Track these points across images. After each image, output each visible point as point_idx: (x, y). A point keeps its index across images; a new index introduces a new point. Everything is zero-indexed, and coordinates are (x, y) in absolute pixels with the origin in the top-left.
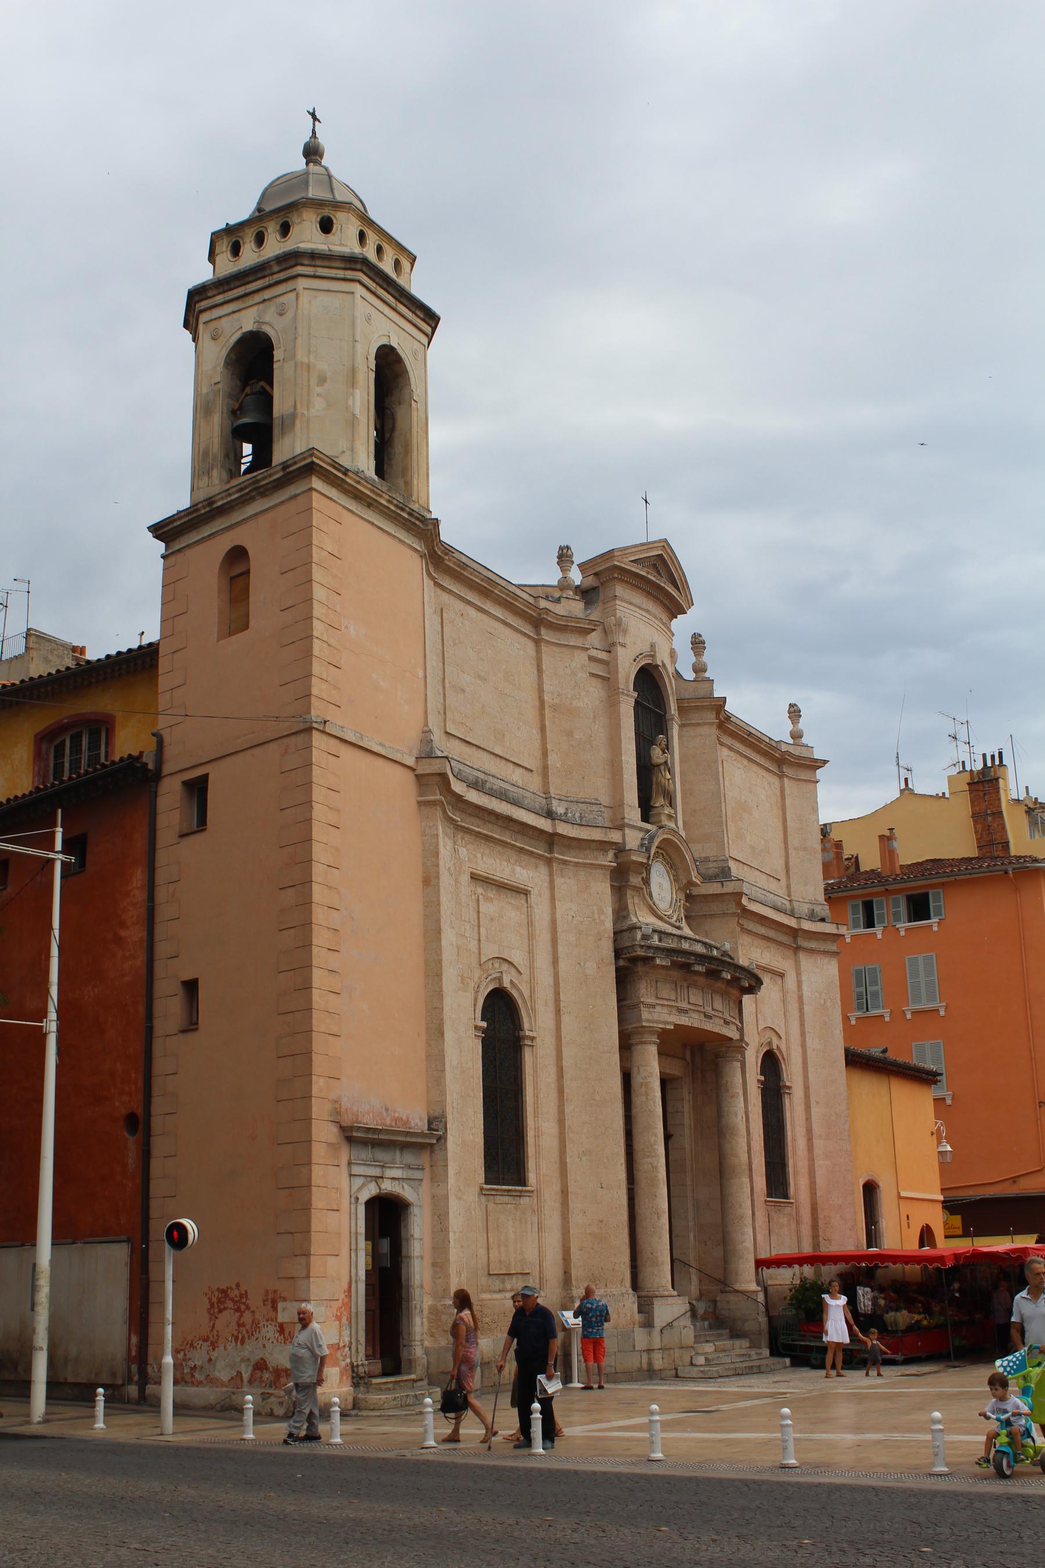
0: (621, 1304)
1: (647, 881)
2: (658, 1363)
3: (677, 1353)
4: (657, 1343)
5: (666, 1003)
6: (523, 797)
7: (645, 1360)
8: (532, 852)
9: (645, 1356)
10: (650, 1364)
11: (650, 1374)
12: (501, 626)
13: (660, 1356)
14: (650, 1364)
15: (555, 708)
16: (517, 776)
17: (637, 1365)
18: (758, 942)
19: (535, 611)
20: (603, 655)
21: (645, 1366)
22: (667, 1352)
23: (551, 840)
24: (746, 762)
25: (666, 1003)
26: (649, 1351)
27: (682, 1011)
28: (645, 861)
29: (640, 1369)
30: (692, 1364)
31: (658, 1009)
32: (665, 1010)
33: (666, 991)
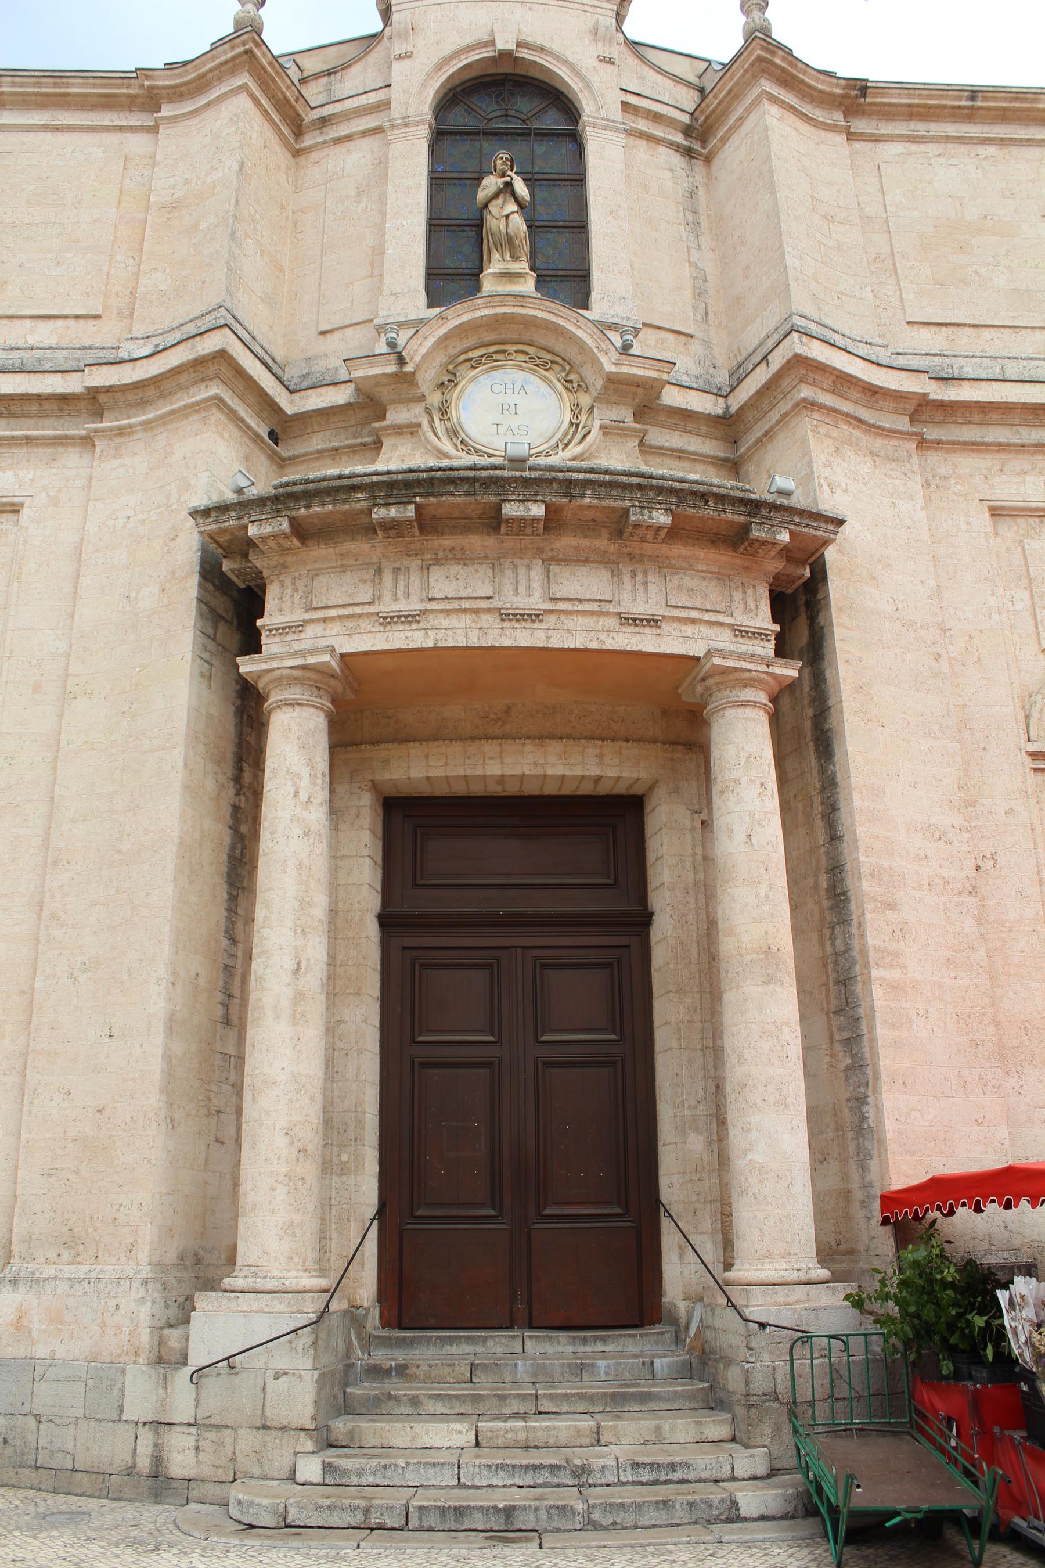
0: (112, 1303)
1: (444, 411)
2: (181, 1461)
3: (247, 1440)
4: (182, 1401)
5: (332, 613)
6: (39, 360)
7: (145, 1449)
8: (27, 438)
9: (146, 1438)
10: (158, 1460)
11: (158, 1484)
12: (48, 136)
13: (190, 1441)
14: (158, 1460)
15: (172, 207)
16: (45, 334)
17: (121, 1457)
18: (1018, 462)
19: (129, 87)
20: (381, 95)
21: (144, 1464)
22: (212, 1435)
23: (95, 402)
24: (992, 150)
25: (332, 613)
26: (157, 1425)
27: (389, 620)
28: (391, 369)
29: (130, 1471)
30: (292, 1478)
31: (310, 631)
32: (336, 628)
33: (339, 589)
